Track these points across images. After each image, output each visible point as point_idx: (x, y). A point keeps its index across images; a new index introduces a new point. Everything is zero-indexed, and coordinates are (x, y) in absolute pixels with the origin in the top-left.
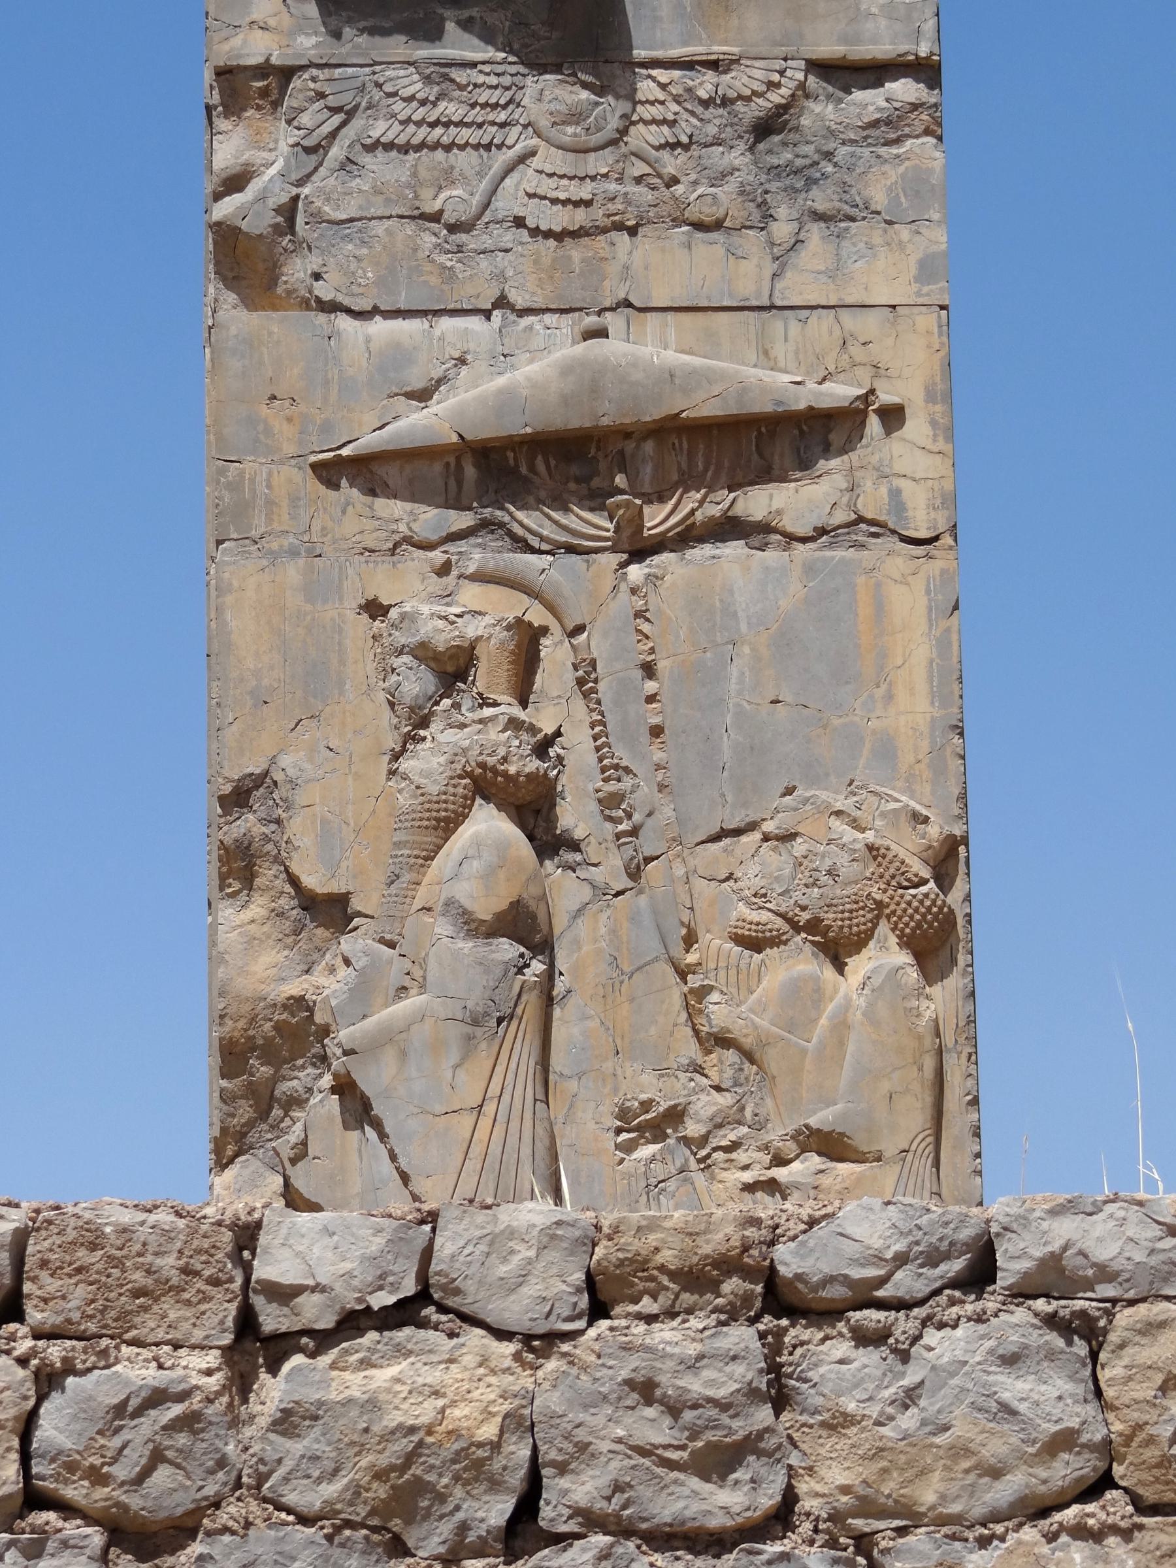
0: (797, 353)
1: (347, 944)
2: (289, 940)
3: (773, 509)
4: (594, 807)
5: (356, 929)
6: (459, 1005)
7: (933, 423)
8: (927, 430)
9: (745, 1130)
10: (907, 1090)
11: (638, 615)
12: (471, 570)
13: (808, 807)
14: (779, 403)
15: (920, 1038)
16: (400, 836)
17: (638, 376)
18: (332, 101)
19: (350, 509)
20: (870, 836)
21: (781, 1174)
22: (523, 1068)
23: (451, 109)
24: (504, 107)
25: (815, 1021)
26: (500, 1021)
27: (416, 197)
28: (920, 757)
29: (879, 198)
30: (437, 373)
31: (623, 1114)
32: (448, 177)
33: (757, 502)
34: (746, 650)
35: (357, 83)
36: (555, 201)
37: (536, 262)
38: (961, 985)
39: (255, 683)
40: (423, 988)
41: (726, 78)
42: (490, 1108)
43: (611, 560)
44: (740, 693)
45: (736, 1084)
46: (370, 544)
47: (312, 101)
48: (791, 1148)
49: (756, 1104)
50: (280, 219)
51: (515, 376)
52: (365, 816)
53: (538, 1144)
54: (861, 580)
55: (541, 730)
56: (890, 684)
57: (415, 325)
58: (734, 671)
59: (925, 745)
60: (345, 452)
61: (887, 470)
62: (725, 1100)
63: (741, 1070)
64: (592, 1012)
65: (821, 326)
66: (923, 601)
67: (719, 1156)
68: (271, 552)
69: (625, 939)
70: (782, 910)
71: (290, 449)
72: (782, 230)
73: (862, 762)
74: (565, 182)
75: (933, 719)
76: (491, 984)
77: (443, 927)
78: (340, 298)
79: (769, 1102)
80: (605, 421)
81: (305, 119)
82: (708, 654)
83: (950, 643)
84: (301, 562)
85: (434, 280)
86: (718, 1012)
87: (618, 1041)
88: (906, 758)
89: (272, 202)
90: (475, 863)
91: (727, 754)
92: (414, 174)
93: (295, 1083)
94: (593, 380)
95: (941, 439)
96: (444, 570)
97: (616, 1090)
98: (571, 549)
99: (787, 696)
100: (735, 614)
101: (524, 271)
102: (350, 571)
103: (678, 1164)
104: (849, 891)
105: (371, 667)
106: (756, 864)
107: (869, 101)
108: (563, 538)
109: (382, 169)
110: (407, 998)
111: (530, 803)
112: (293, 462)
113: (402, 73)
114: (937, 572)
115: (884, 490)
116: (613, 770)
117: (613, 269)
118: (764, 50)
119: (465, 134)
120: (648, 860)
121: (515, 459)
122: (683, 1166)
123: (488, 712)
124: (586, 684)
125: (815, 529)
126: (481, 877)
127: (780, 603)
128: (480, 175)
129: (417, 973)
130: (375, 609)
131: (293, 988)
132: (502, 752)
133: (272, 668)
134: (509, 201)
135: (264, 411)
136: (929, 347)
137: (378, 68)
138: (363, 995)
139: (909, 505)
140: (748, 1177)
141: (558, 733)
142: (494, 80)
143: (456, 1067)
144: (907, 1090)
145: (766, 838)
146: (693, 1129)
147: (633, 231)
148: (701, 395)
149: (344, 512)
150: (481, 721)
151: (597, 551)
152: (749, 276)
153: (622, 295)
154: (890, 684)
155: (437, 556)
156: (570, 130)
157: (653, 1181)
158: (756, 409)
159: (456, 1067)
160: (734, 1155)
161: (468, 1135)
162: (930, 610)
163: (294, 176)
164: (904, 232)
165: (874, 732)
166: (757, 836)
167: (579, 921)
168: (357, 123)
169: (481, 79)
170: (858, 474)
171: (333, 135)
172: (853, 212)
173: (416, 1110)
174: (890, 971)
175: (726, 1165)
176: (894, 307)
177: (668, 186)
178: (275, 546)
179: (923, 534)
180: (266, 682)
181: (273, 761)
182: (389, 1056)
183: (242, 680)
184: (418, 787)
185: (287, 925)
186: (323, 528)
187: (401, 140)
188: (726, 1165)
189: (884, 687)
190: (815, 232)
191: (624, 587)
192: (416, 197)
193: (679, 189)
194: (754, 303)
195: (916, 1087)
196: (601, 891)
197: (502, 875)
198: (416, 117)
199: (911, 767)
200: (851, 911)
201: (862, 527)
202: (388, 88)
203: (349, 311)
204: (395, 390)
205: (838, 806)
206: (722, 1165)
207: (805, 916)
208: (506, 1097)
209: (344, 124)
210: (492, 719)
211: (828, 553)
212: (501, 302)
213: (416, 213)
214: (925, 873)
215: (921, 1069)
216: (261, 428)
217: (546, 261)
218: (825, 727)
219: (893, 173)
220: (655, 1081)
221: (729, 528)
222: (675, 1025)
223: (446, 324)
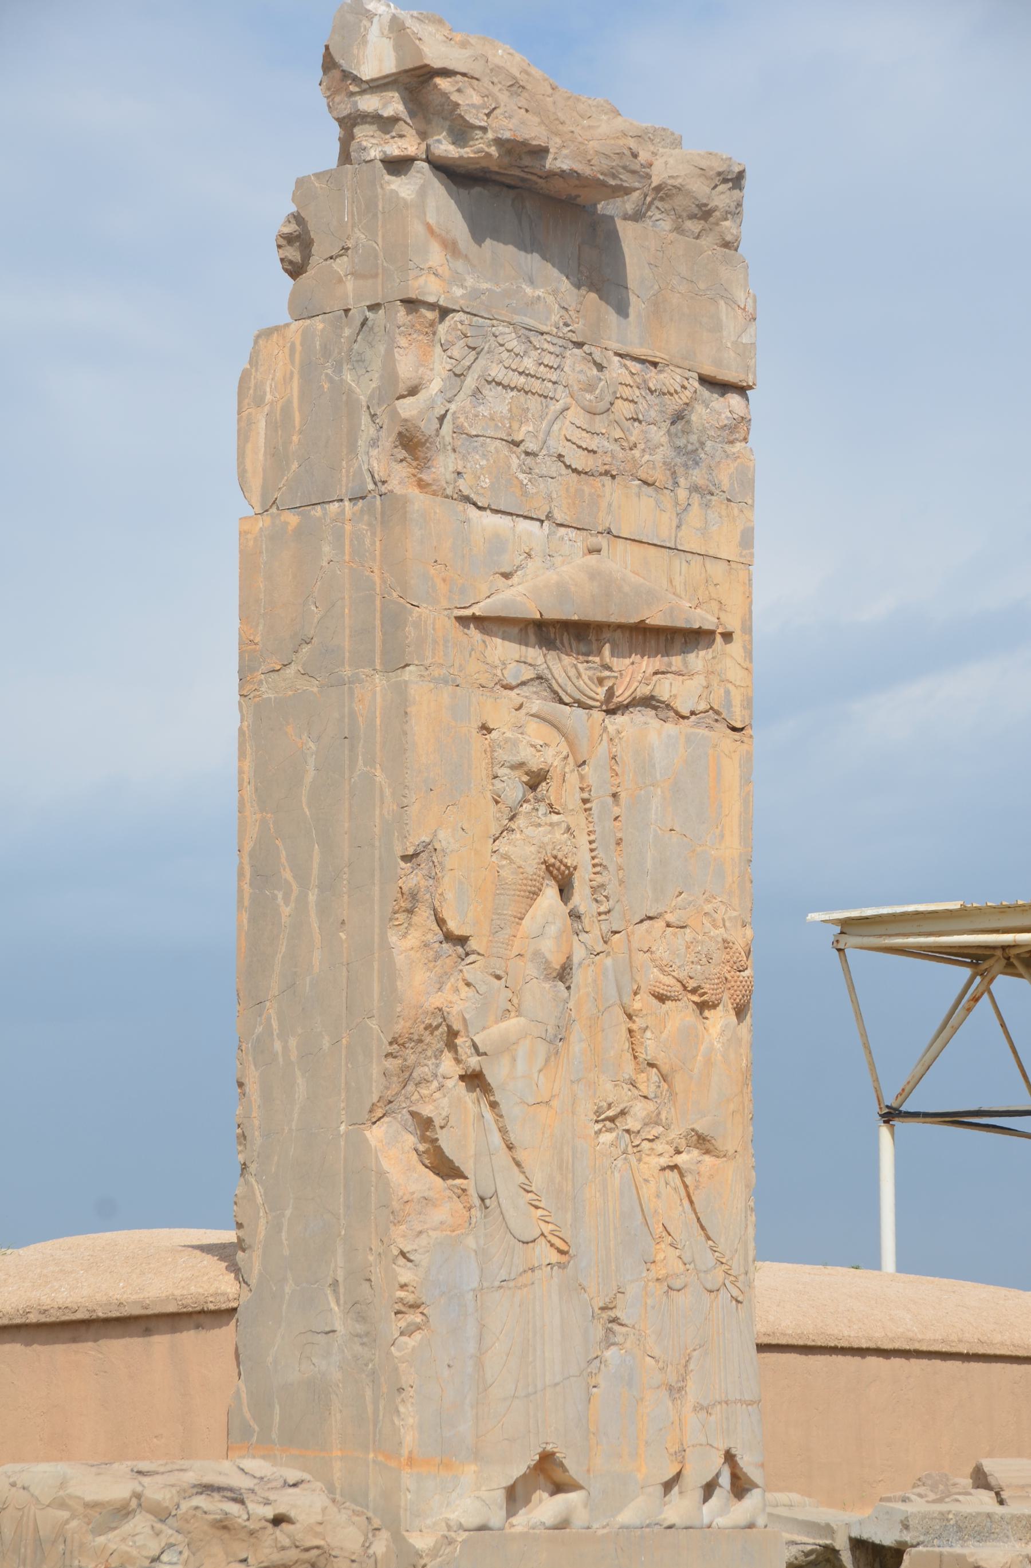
1: (470, 972)
2: (431, 965)
9: (661, 1129)
12: (533, 711)
14: (687, 621)
30: (517, 563)
31: (598, 1112)
40: (519, 1013)
46: (483, 682)
62: (651, 1106)
63: (659, 1087)
67: (646, 1145)
71: (445, 604)
77: (531, 970)
86: (650, 1047)
93: (426, 1069)
101: (556, 491)
106: (665, 944)
108: (578, 696)
112: (446, 613)
115: (722, 691)
116: (599, 867)
123: (555, 818)
129: (515, 1001)
130: (485, 729)
140: (664, 1161)
143: (540, 1071)
146: (631, 1123)
147: (613, 477)
150: (551, 825)
151: (590, 708)
159: (540, 1071)
182: (505, 1060)
184: (519, 867)
190: (696, 498)
194: (668, 545)
203: (475, 504)
207: (691, 984)
210: (558, 824)
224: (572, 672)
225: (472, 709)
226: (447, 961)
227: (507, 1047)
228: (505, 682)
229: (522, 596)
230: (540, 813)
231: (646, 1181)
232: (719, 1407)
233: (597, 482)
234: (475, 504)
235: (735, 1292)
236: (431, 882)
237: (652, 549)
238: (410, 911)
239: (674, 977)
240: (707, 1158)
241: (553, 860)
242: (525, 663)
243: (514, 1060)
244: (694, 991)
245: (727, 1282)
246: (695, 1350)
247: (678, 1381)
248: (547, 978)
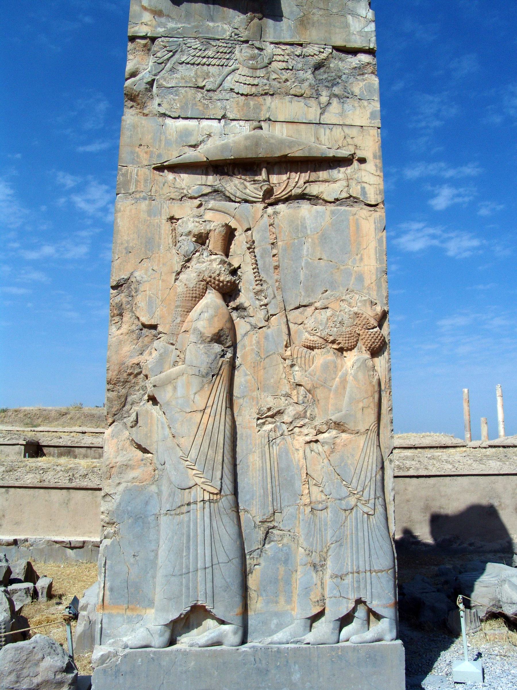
0: (328, 139)
2: (135, 342)
3: (320, 191)
4: (252, 295)
5: (160, 338)
6: (197, 370)
7: (376, 166)
8: (374, 168)
9: (307, 420)
10: (369, 406)
11: (271, 225)
13: (332, 298)
14: (323, 153)
15: (373, 386)
16: (178, 303)
17: (272, 141)
18: (168, 48)
19: (166, 184)
20: (355, 309)
21: (320, 437)
22: (222, 394)
23: (210, 53)
24: (229, 53)
25: (334, 379)
26: (213, 376)
27: (196, 81)
28: (372, 281)
29: (356, 90)
30: (200, 139)
32: (207, 75)
34: (310, 240)
35: (178, 43)
36: (245, 84)
37: (237, 104)
38: (387, 366)
39: (127, 245)
41: (305, 50)
42: (208, 411)
43: (261, 206)
44: (307, 255)
45: (303, 403)
46: (173, 197)
47: (162, 49)
48: (325, 427)
49: (312, 411)
50: (148, 86)
52: (165, 295)
53: (227, 425)
54: (351, 218)
55: (233, 265)
56: (362, 255)
57: (194, 123)
58: (305, 247)
59: (374, 277)
60: (165, 164)
61: (360, 181)
62: (300, 408)
63: (306, 397)
64: (249, 373)
66: (373, 227)
67: (297, 430)
68: (136, 198)
69: (262, 345)
70: (322, 336)
71: (146, 163)
72: (324, 99)
73: (352, 282)
74: (249, 78)
75: (377, 268)
76: (210, 361)
78: (167, 113)
79: (316, 409)
80: (260, 156)
81: (159, 55)
82: (296, 241)
83: (383, 241)
84: (147, 202)
85: (201, 108)
87: (259, 384)
88: (367, 282)
89: (145, 81)
90: (206, 314)
91: (302, 278)
92: (196, 74)
93: (135, 396)
94: (257, 143)
95: (379, 171)
96: (200, 206)
97: (258, 403)
98: (246, 201)
99: (324, 257)
100: (306, 227)
101: (233, 107)
102: (165, 206)
103: (281, 433)
104: (348, 329)
105: (170, 241)
107: (354, 61)
108: (245, 197)
110: (177, 366)
111: (228, 293)
113: (193, 41)
114: (378, 216)
115: (359, 187)
116: (260, 282)
117: (264, 108)
118: (318, 42)
119: (214, 61)
120: (273, 315)
121: (227, 169)
122: (282, 433)
123: (213, 257)
124: (251, 248)
125: (335, 199)
126: (208, 320)
127: (322, 224)
128: (219, 75)
129: (182, 356)
131: (136, 361)
132: (218, 272)
133: (133, 240)
134: (229, 83)
135: (137, 149)
136: (374, 140)
137: (185, 39)
139: (368, 192)
140: (308, 438)
141: (239, 267)
142: (225, 45)
143: (195, 393)
144: (369, 406)
145: (316, 309)
146: (287, 418)
148: (295, 149)
149: (164, 185)
150: (210, 261)
152: (312, 112)
153: (267, 116)
154: (362, 255)
155: (197, 202)
156: (251, 62)
157: (271, 439)
158: (315, 155)
159: (195, 393)
160: (302, 430)
161: (199, 422)
162: (376, 230)
163: (154, 73)
164: (365, 103)
165: (356, 272)
166: (313, 308)
167: (245, 338)
168: (177, 56)
169: (221, 44)
170: (350, 181)
171: (168, 59)
172: (348, 95)
173: (179, 410)
174: (363, 361)
175: (299, 434)
176: (362, 126)
177: (285, 82)
178: (138, 196)
179: (373, 203)
180: (131, 245)
181: (132, 274)
182: (169, 388)
183: (122, 244)
185: (135, 336)
186: (156, 191)
187: (192, 62)
188: (299, 434)
189: (359, 256)
190: (335, 102)
191: (266, 216)
192: (196, 81)
193: (288, 83)
195: (372, 405)
196: (254, 327)
197: (216, 319)
198: (198, 55)
199: (369, 285)
200: (349, 337)
201: (352, 200)
202: (188, 45)
203: (170, 117)
204: (185, 144)
205: (344, 298)
206: (297, 434)
207: (331, 339)
208: (215, 406)
209: (172, 56)
210: (215, 260)
211: (339, 208)
212: (224, 117)
213: (196, 86)
214: (376, 324)
215: (374, 398)
216: (135, 155)
217: (241, 104)
218: (338, 269)
219: (361, 84)
220: (272, 400)
222: (281, 379)
223: (205, 123)
224: (241, 187)
225: (163, 211)
226: (146, 339)
227: (170, 381)
228: (189, 196)
230: (204, 256)
231: (297, 450)
232: (350, 575)
233: (261, 99)
234: (170, 117)
235: (366, 509)
236: (130, 298)
237: (303, 126)
238: (121, 315)
239: (317, 336)
240: (344, 435)
241: (209, 279)
242: (206, 185)
243: (175, 388)
244: (333, 342)
245: (358, 504)
246: (332, 544)
247: (320, 561)
248: (203, 342)
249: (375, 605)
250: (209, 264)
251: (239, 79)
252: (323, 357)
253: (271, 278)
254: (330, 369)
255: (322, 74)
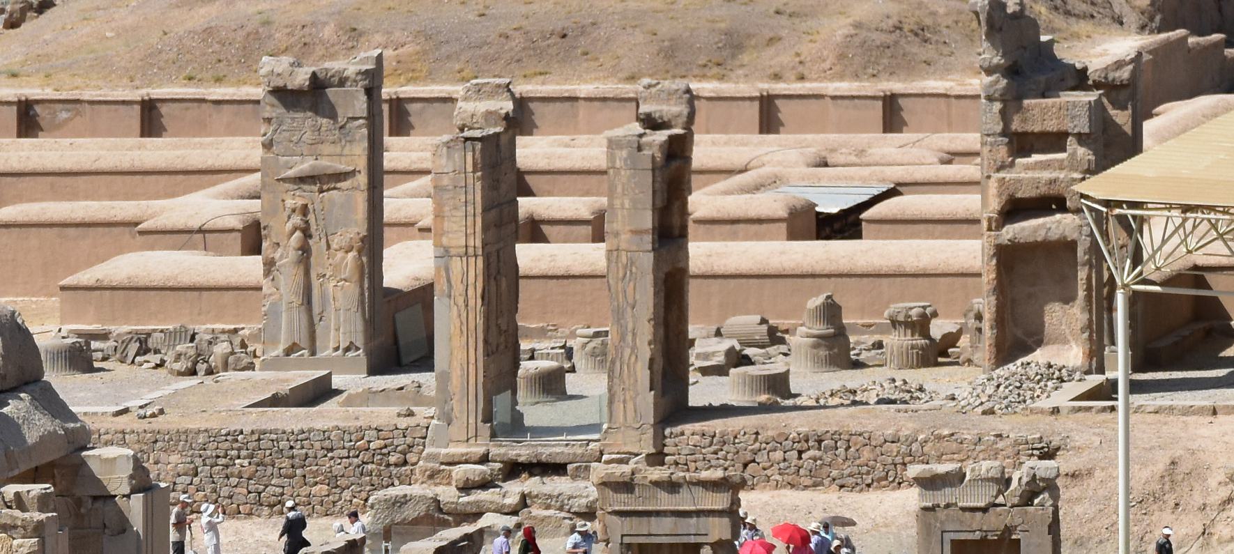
33: (338, 185)
51: (304, 166)
65: (349, 158)
109: (286, 134)
138: (281, 257)
221: (335, 188)
229: (290, 173)
249: (359, 344)
250: (297, 219)
251: (308, 137)
252: (340, 255)
253: (322, 223)
254: (343, 258)
255: (343, 131)
